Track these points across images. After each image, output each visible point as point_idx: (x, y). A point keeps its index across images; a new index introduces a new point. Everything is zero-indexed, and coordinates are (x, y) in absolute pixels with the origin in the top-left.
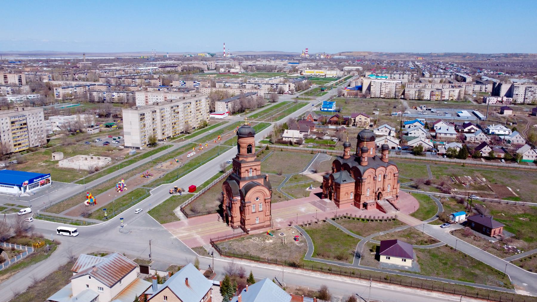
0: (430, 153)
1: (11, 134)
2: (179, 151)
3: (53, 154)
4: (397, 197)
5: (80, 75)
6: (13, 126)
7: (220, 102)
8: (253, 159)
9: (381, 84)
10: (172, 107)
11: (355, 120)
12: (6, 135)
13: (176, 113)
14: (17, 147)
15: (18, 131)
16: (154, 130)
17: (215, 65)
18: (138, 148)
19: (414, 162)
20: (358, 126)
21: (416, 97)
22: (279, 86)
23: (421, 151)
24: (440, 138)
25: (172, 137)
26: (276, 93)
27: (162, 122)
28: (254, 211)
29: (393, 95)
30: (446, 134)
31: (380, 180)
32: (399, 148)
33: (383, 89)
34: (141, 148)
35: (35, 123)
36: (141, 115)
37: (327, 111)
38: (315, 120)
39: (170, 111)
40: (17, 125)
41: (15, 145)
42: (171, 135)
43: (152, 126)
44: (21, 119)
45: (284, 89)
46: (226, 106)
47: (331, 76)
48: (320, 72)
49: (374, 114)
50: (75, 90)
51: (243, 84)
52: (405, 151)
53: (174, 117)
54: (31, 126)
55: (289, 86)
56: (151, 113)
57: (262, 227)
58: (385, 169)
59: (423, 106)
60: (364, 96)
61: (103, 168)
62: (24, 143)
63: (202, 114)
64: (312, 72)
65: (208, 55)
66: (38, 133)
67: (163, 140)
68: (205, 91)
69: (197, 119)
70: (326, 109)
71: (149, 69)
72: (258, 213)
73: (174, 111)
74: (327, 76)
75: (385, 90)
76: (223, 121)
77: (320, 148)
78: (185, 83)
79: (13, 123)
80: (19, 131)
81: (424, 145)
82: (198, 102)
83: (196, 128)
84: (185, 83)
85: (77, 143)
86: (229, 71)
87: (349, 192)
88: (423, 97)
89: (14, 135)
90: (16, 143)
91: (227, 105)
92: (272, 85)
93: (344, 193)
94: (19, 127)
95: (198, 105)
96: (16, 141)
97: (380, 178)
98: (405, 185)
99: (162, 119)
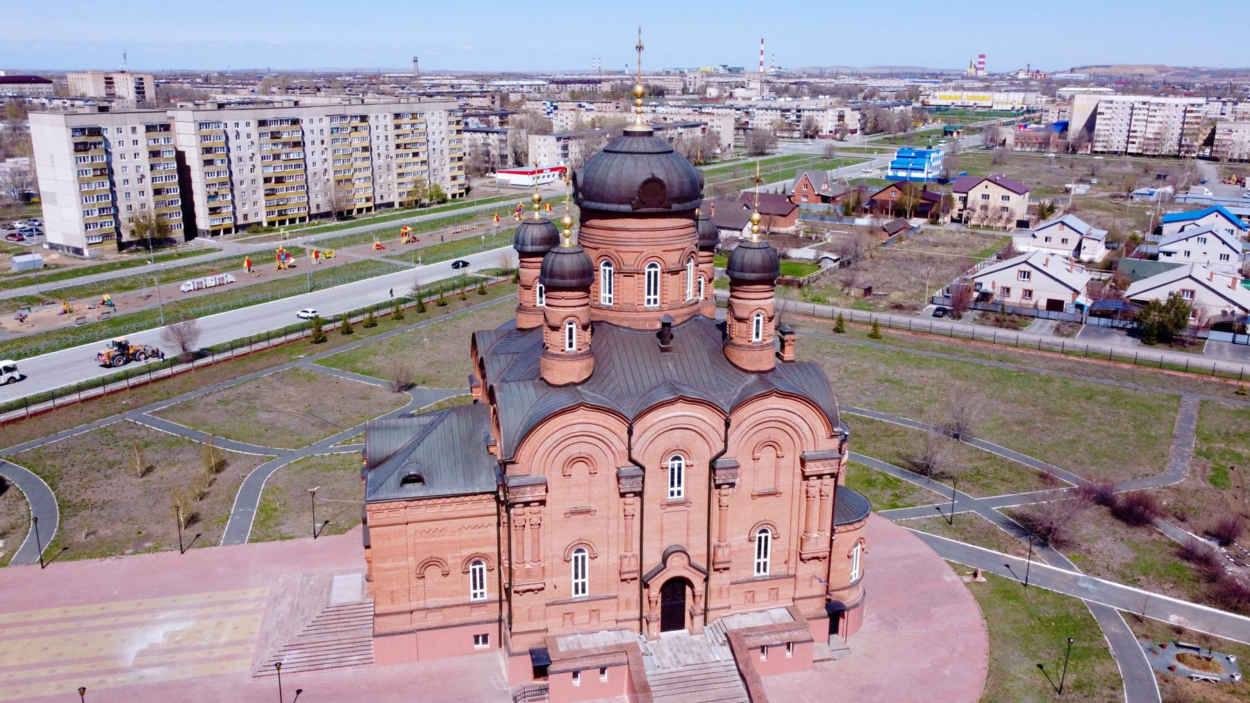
0: (1228, 336)
2: (190, 270)
4: (835, 613)
7: (542, 138)
9: (1132, 109)
10: (262, 123)
11: (965, 200)
13: (285, 144)
16: (157, 192)
18: (78, 251)
19: (1132, 377)
20: (973, 222)
22: (806, 113)
23: (1180, 324)
25: (265, 224)
27: (210, 168)
29: (1170, 146)
32: (1080, 307)
33: (1139, 127)
34: (86, 253)
36: (75, 130)
38: (825, 199)
39: (255, 136)
42: (263, 218)
43: (148, 180)
46: (560, 151)
47: (1008, 107)
48: (978, 98)
49: (1068, 191)
52: (1103, 321)
56: (141, 130)
58: (717, 421)
60: (1073, 149)
63: (423, 162)
64: (956, 98)
68: (565, 121)
69: (400, 175)
71: (522, 86)
73: (275, 135)
75: (1146, 130)
78: (556, 108)
81: (1203, 296)
82: (406, 120)
83: (397, 205)
84: (556, 108)
87: (453, 560)
91: (565, 148)
92: (784, 111)
98: (984, 507)
99: (209, 157)
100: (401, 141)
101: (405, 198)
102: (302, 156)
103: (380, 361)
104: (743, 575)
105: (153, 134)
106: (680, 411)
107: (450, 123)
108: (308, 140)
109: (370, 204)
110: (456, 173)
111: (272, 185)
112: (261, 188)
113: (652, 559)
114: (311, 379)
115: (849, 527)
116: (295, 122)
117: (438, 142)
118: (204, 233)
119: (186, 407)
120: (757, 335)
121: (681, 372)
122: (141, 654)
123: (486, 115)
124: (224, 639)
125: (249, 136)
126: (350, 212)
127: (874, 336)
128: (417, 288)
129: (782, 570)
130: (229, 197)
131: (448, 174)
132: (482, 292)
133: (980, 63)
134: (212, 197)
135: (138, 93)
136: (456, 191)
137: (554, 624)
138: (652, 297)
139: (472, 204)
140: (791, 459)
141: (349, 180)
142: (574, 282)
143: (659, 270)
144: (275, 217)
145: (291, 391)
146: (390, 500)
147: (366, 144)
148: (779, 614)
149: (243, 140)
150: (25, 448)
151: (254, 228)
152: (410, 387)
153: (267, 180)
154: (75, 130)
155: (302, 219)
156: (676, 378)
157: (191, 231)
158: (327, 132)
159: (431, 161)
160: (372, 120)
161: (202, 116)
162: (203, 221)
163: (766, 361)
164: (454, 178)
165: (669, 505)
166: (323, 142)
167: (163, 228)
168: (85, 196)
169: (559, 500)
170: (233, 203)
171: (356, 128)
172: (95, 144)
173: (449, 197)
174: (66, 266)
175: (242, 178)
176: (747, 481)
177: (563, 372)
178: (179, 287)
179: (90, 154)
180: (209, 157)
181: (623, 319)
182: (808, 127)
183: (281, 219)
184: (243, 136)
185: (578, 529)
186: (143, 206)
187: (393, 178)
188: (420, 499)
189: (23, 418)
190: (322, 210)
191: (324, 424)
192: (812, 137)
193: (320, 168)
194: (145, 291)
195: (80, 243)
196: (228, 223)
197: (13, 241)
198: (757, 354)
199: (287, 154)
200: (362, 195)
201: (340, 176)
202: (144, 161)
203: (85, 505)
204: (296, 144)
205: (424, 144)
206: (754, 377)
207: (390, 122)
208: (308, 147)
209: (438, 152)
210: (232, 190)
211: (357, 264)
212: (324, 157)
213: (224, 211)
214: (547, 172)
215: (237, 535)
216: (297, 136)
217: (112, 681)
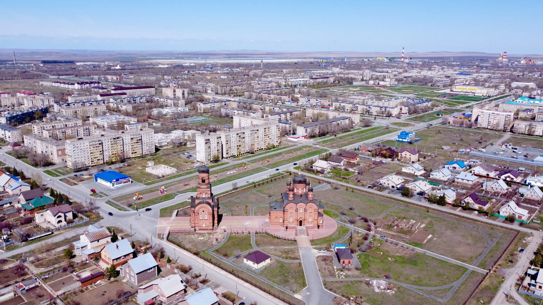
1: (130, 146)
3: (148, 162)
5: (236, 87)
7: (300, 127)
8: (205, 187)
10: (237, 134)
12: (128, 146)
14: (134, 154)
16: (218, 150)
17: (370, 76)
20: (402, 161)
21: (527, 131)
22: (388, 109)
24: (458, 183)
26: (385, 115)
28: (201, 218)
29: (501, 127)
30: (463, 179)
31: (301, 212)
33: (491, 120)
35: (148, 139)
37: (402, 141)
38: (369, 151)
39: (236, 137)
40: (135, 140)
41: (132, 153)
42: (236, 154)
44: (137, 136)
45: (392, 113)
46: (305, 131)
48: (472, 90)
49: (443, 148)
50: (213, 105)
51: (356, 105)
53: (240, 141)
55: (401, 109)
56: (216, 138)
57: (207, 230)
59: (508, 145)
61: (168, 175)
64: (464, 89)
65: (385, 59)
67: (227, 158)
69: (265, 142)
70: (401, 140)
72: (204, 221)
73: (240, 136)
74: (476, 95)
75: (494, 122)
76: (294, 144)
77: (334, 179)
78: (309, 100)
80: (136, 144)
82: (267, 129)
85: (173, 154)
86: (378, 84)
87: (279, 217)
88: (534, 132)
89: (132, 147)
91: (306, 130)
93: (274, 217)
94: (136, 142)
95: (267, 131)
97: (301, 211)
100: (266, 134)
101: (266, 147)
103: (265, 191)
106: (301, 204)
110: (278, 140)
111: (238, 147)
112: (236, 148)
113: (298, 218)
114: (255, 194)
116: (244, 133)
118: (225, 158)
119: (238, 198)
123: (286, 113)
127: (353, 191)
131: (276, 140)
132: (283, 177)
133: (504, 55)
134: (227, 151)
136: (278, 144)
137: (288, 224)
139: (281, 149)
140: (313, 209)
145: (253, 196)
148: (312, 225)
151: (234, 156)
152: (271, 196)
153: (237, 146)
157: (223, 158)
160: (259, 131)
161: (226, 134)
162: (225, 156)
163: (311, 199)
167: (218, 158)
168: (206, 152)
169: (289, 211)
176: (308, 211)
177: (290, 199)
178: (226, 173)
182: (388, 114)
185: (291, 214)
187: (263, 143)
191: (259, 202)
192: (389, 116)
193: (248, 142)
194: (221, 174)
196: (230, 156)
200: (256, 147)
202: (216, 144)
204: (244, 138)
207: (263, 130)
211: (258, 168)
214: (301, 137)
215: (252, 215)
216: (244, 136)
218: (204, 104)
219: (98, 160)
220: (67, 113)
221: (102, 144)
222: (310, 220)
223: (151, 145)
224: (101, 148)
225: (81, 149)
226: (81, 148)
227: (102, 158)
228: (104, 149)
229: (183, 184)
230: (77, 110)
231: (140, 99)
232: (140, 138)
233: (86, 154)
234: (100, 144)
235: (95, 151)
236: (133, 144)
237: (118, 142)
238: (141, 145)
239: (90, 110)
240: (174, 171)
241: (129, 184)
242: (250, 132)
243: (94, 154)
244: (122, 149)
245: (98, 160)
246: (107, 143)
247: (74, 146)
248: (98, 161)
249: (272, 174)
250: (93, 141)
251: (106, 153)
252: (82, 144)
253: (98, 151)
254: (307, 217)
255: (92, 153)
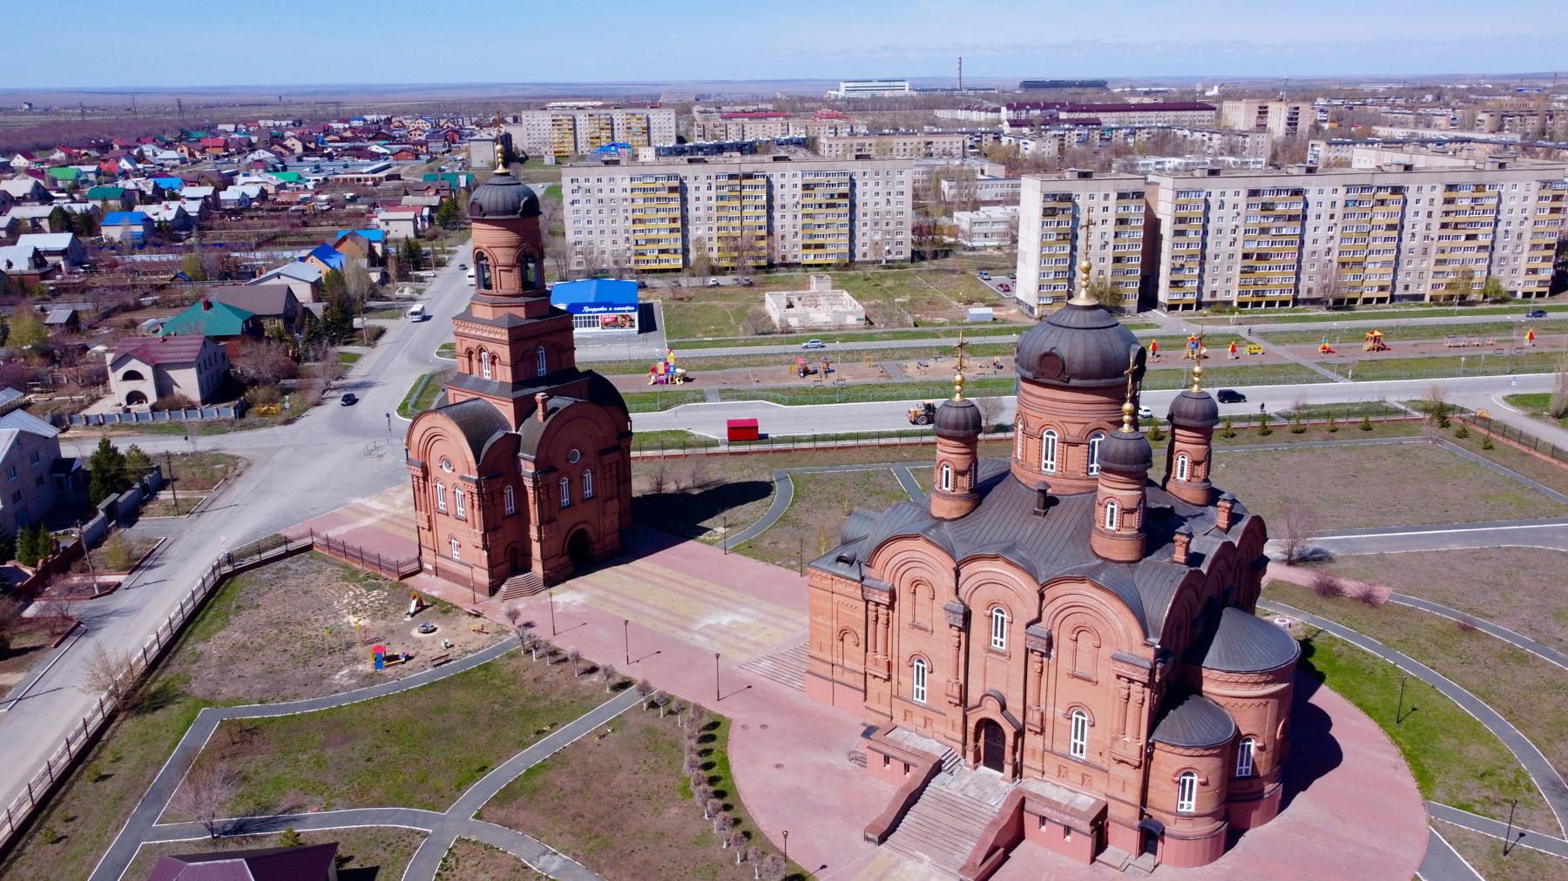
1: (800, 216)
6: (807, 195)
10: (1254, 193)
12: (789, 216)
13: (1278, 217)
14: (812, 252)
15: (818, 211)
16: (1117, 260)
18: (1031, 309)
25: (1235, 304)
27: (1181, 239)
35: (882, 199)
36: (1046, 196)
39: (1242, 207)
40: (820, 196)
41: (806, 247)
42: (1234, 297)
43: (1111, 246)
54: (865, 204)
56: (1113, 196)
61: (815, 330)
62: (833, 245)
63: (1481, 248)
66: (885, 228)
69: (1439, 262)
73: (1266, 207)
79: (806, 187)
80: (823, 210)
83: (1427, 299)
89: (807, 221)
90: (809, 242)
94: (824, 201)
96: (812, 236)
99: (1181, 227)
100: (1450, 219)
101: (1442, 291)
102: (1298, 231)
104: (1058, 747)
105: (1124, 202)
106: (996, 568)
107: (1541, 198)
108: (1311, 213)
109: (1386, 294)
110: (1533, 265)
111: (1252, 262)
112: (1239, 263)
115: (1171, 748)
116: (1297, 192)
117: (1515, 224)
120: (1111, 523)
121: (1034, 537)
122: (709, 626)
124: (754, 638)
125: (1235, 206)
126: (1354, 301)
128: (1298, 408)
129: (1097, 760)
130: (1197, 271)
131: (1523, 264)
134: (1174, 270)
135: (1289, 124)
136: (1534, 288)
138: (1049, 462)
140: (1106, 652)
141: (1360, 263)
142: (947, 432)
143: (1056, 438)
144: (1248, 298)
146: (823, 570)
147: (1395, 220)
149: (1228, 211)
150: (809, 471)
153: (1246, 256)
154: (1046, 196)
155: (1284, 303)
156: (1023, 541)
157: (1148, 300)
158: (1340, 204)
159: (1498, 246)
160: (1411, 195)
162: (1164, 294)
164: (1535, 271)
165: (990, 651)
166: (1332, 216)
168: (1043, 258)
170: (1200, 277)
171: (1382, 202)
172: (1063, 210)
173: (1519, 295)
174: (1011, 322)
175: (1217, 252)
179: (1057, 219)
180: (1181, 227)
181: (1023, 476)
183: (1256, 302)
184: (1229, 206)
186: (1101, 272)
187: (1429, 264)
188: (841, 577)
189: (832, 448)
190: (1314, 296)
193: (1322, 246)
195: (1033, 302)
196: (1191, 298)
197: (1000, 291)
198: (1106, 541)
199: (1279, 229)
200: (1375, 281)
201: (1346, 257)
202: (1110, 228)
203: (795, 524)
204: (1291, 218)
205: (1489, 224)
206: (1099, 562)
207: (1439, 194)
208: (1311, 223)
209: (1512, 238)
210: (1202, 265)
212: (1331, 233)
213: (1188, 285)
216: (1297, 208)
217: (680, 634)
218: (1330, 144)
219: (662, 251)
220: (834, 148)
221: (681, 190)
222: (1083, 745)
223: (891, 226)
224: (676, 204)
225: (601, 201)
226: (601, 196)
227: (679, 245)
228: (692, 213)
229: (796, 367)
230: (867, 141)
231: (1126, 135)
232: (845, 189)
233: (621, 225)
234: (672, 190)
235: (650, 214)
236: (809, 210)
237: (745, 192)
238: (846, 220)
239: (908, 147)
240: (851, 320)
241: (629, 336)
242: (1341, 196)
243: (649, 225)
244: (763, 221)
245: (662, 251)
246: (704, 193)
247: (575, 185)
248: (663, 257)
249: (1310, 402)
250: (645, 176)
251: (695, 232)
252: (605, 179)
253: (661, 214)
254: (1054, 712)
255: (641, 221)
